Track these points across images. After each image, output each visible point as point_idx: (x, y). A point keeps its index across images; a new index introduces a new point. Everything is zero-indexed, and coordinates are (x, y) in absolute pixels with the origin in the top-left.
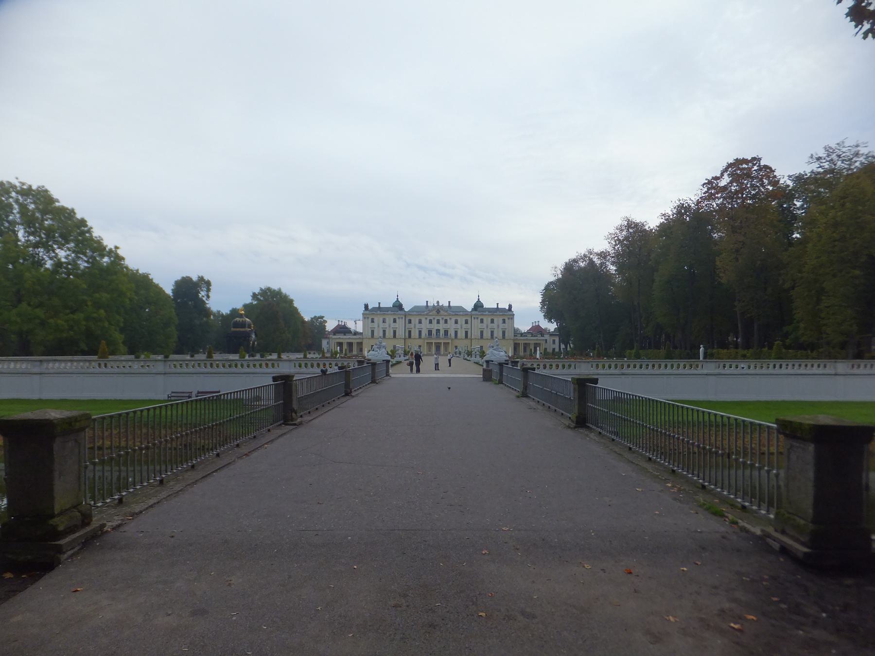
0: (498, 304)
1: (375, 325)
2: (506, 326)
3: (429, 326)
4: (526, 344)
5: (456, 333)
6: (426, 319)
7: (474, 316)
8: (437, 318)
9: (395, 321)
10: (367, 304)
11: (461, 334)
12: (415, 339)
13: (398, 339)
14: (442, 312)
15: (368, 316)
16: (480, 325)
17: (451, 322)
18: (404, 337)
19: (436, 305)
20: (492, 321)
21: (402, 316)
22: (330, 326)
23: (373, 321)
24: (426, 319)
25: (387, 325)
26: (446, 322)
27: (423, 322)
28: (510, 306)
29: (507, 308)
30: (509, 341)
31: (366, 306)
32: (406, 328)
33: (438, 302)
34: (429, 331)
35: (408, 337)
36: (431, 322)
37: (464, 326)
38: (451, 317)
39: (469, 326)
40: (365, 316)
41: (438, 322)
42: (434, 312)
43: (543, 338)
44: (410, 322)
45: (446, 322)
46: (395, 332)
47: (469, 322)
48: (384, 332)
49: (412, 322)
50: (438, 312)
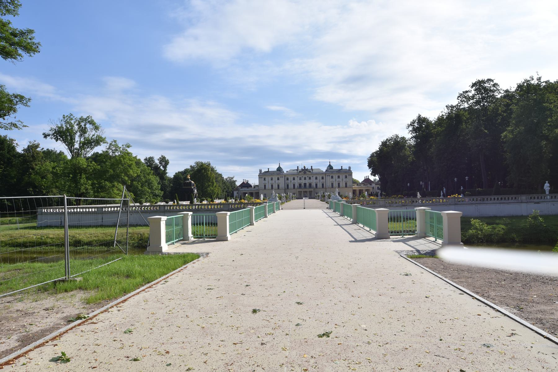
1: (266, 182)
2: (347, 179)
3: (299, 181)
4: (360, 190)
5: (316, 185)
6: (298, 177)
9: (278, 179)
10: (261, 170)
11: (320, 185)
12: (291, 189)
13: (280, 189)
14: (307, 172)
15: (262, 177)
16: (331, 180)
18: (284, 188)
19: (303, 168)
20: (339, 177)
22: (238, 184)
23: (265, 180)
24: (298, 177)
25: (273, 181)
26: (310, 178)
27: (296, 179)
28: (350, 168)
29: (348, 169)
31: (261, 171)
32: (286, 182)
34: (299, 184)
35: (286, 188)
36: (300, 179)
37: (321, 180)
39: (324, 180)
41: (305, 179)
43: (371, 186)
44: (288, 179)
45: (310, 178)
46: (278, 186)
47: (324, 178)
48: (272, 186)
49: (289, 179)
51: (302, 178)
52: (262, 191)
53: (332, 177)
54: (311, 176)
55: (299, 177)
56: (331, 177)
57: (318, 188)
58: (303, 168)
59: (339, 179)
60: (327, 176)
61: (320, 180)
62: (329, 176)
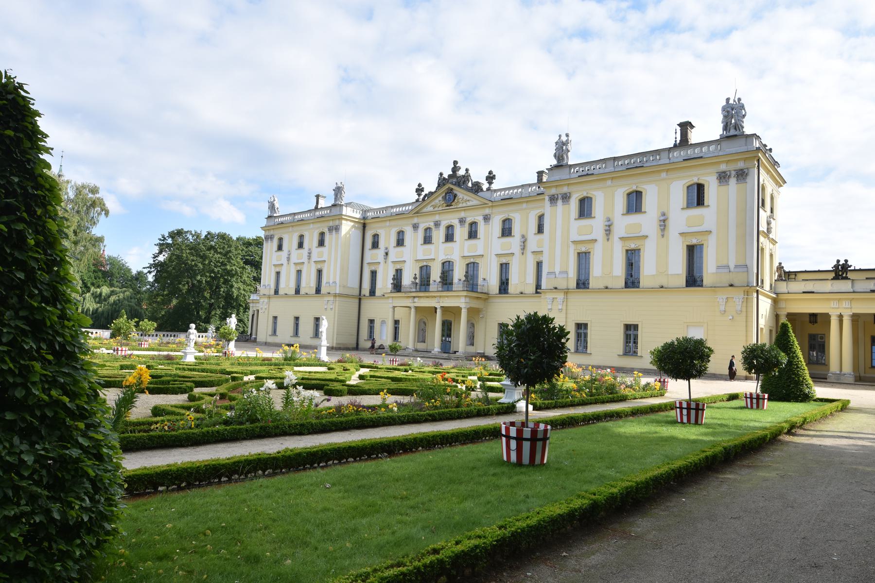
0: (685, 127)
3: (423, 252)
6: (415, 227)
7: (553, 191)
13: (324, 295)
16: (578, 229)
17: (490, 231)
23: (280, 248)
26: (473, 234)
30: (721, 297)
32: (366, 261)
33: (455, 169)
35: (367, 294)
38: (487, 211)
40: (267, 233)
42: (439, 200)
45: (473, 234)
53: (585, 208)
54: (480, 219)
55: (422, 227)
56: (574, 204)
57: (511, 289)
59: (635, 218)
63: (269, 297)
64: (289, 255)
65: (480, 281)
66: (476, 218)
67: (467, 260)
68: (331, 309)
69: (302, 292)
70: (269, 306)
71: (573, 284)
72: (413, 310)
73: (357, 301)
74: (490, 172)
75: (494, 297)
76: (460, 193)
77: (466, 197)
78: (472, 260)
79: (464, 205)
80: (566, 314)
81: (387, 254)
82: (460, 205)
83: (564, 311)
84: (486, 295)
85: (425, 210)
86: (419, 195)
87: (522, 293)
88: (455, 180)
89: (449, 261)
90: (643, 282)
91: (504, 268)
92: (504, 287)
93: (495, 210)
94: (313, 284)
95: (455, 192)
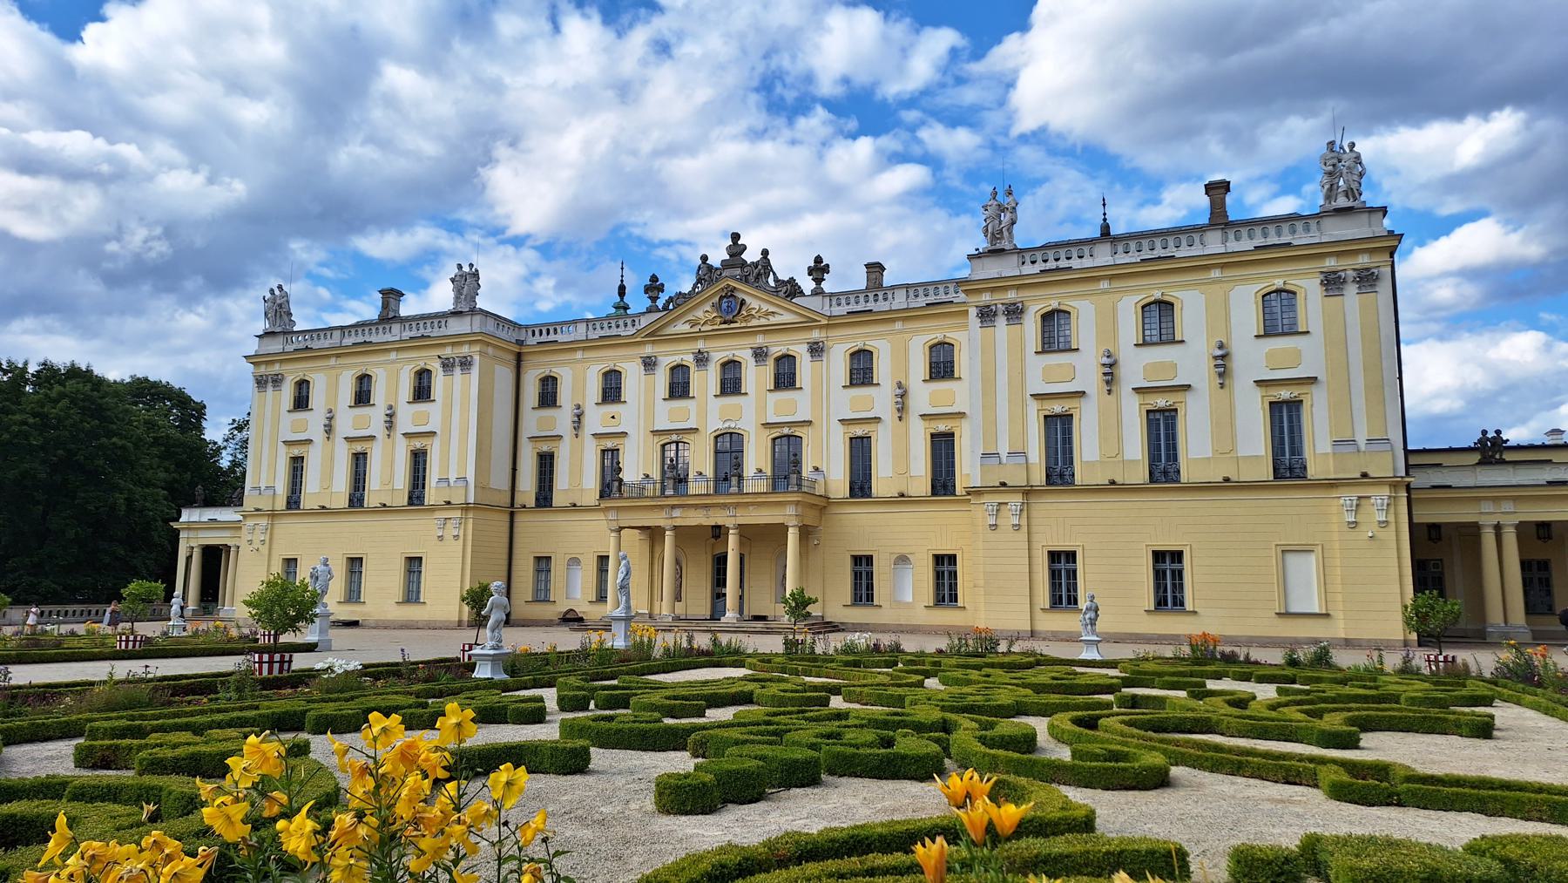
1: (313, 420)
3: (669, 415)
6: (649, 364)
7: (986, 298)
8: (720, 352)
9: (422, 392)
13: (433, 509)
15: (276, 368)
21: (465, 350)
23: (301, 402)
26: (785, 378)
33: (736, 249)
35: (532, 502)
36: (679, 388)
38: (815, 335)
40: (262, 370)
41: (731, 384)
42: (704, 312)
45: (785, 378)
49: (565, 394)
50: (730, 308)
51: (696, 377)
52: (264, 522)
54: (801, 351)
56: (1031, 326)
58: (718, 256)
60: (986, 315)
61: (903, 394)
62: (1015, 313)
63: (273, 515)
64: (330, 419)
65: (807, 471)
66: (791, 348)
67: (773, 431)
68: (456, 537)
69: (372, 499)
70: (271, 534)
71: (1039, 477)
72: (669, 537)
73: (506, 518)
74: (818, 260)
75: (841, 503)
76: (755, 302)
77: (765, 307)
78: (786, 431)
79: (763, 321)
80: (1029, 533)
81: (579, 416)
82: (754, 322)
83: (1025, 529)
84: (824, 500)
85: (671, 330)
86: (654, 299)
87: (903, 495)
88: (738, 271)
89: (731, 433)
90: (1189, 471)
91: (860, 450)
92: (860, 486)
93: (832, 333)
94: (402, 481)
95: (741, 296)
